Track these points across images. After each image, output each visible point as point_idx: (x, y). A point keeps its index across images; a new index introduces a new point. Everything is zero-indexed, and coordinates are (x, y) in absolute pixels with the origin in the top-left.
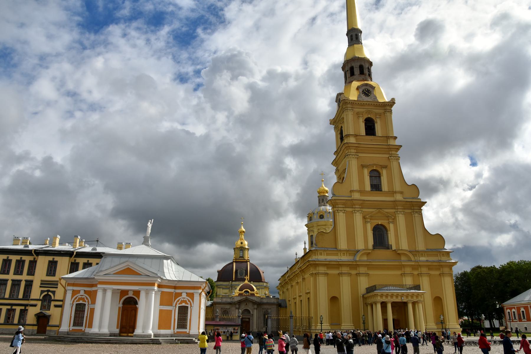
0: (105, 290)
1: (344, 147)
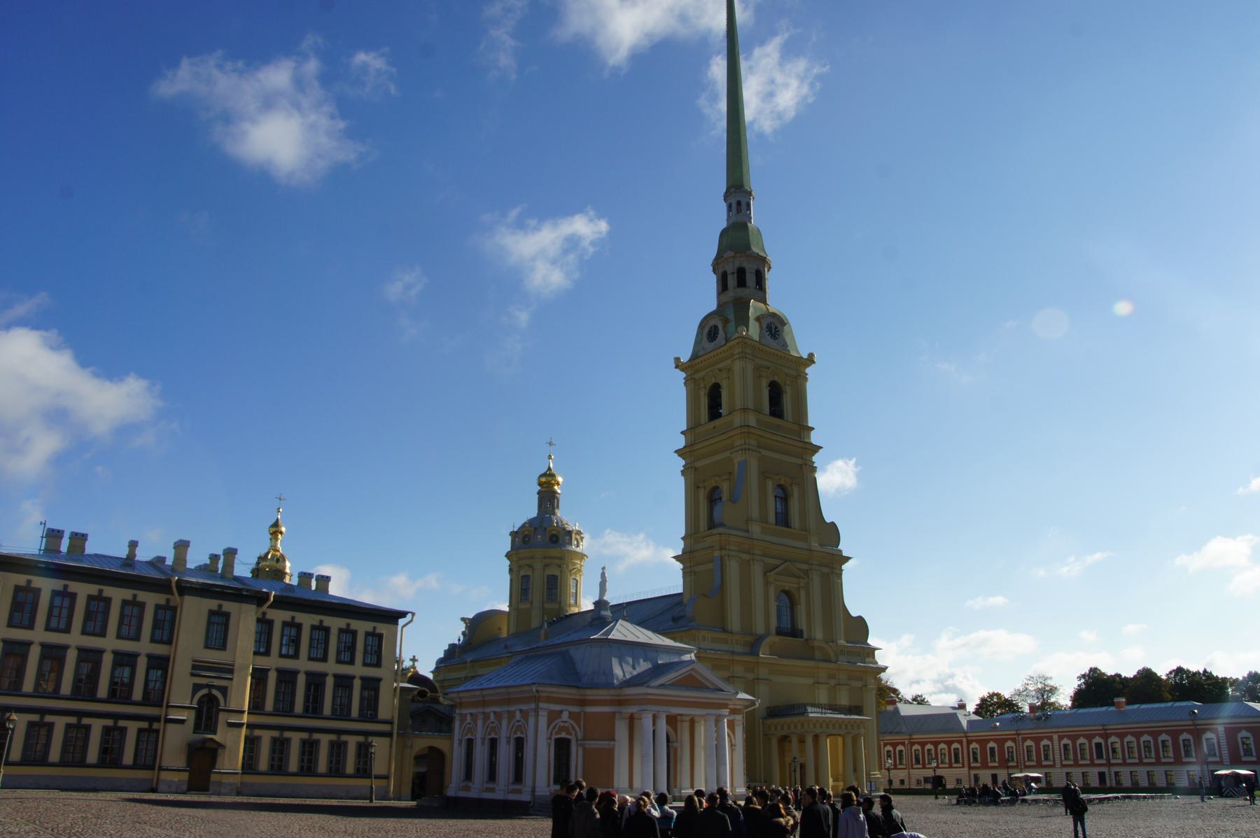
0: (655, 718)
1: (739, 432)
